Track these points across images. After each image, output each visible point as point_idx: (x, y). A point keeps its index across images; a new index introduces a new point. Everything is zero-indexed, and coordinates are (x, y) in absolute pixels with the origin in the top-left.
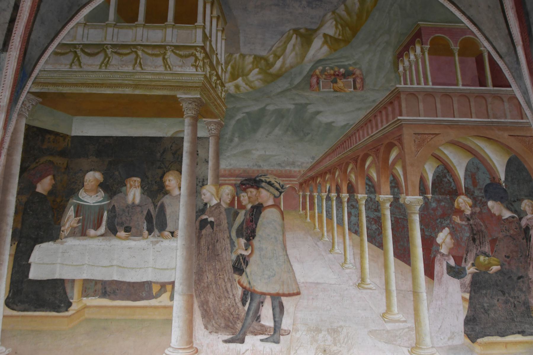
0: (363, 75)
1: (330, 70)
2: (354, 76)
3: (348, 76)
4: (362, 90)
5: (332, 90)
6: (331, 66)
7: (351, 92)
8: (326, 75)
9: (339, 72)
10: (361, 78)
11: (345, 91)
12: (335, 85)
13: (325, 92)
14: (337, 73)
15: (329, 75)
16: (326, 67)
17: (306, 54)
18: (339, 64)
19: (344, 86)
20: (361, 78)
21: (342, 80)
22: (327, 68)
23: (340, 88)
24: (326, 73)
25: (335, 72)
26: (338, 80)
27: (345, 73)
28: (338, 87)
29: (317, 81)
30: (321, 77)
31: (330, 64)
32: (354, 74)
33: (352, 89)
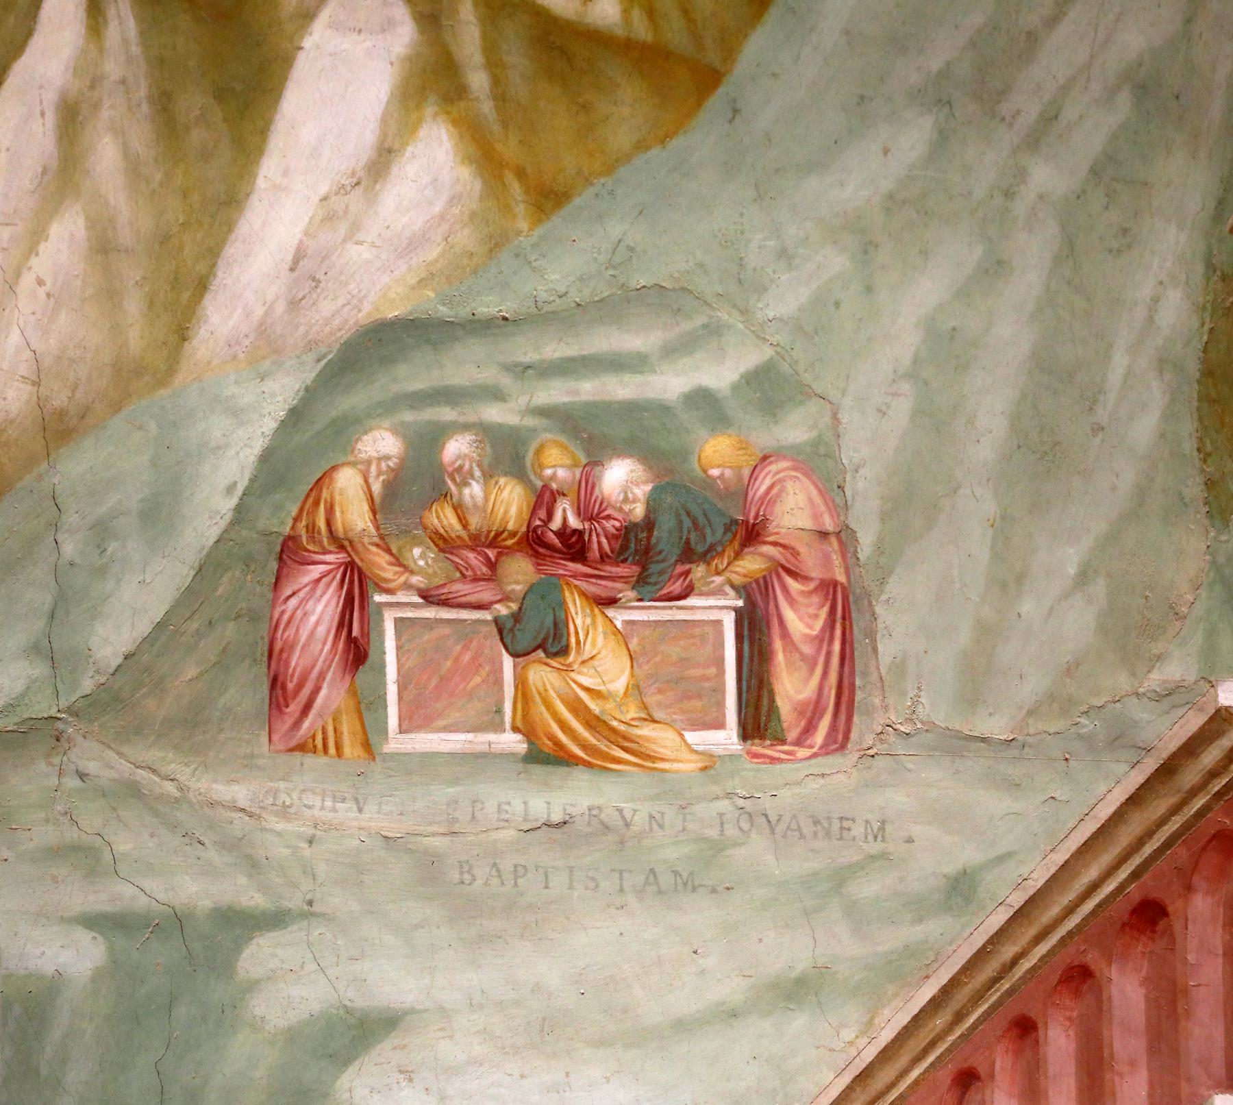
0: (844, 537)
1: (488, 476)
2: (751, 564)
3: (688, 555)
4: (839, 741)
5: (511, 741)
6: (494, 414)
7: (710, 763)
8: (444, 544)
9: (591, 510)
10: (829, 588)
11: (645, 756)
12: (542, 675)
13: (427, 759)
14: (566, 514)
15: (477, 541)
16: (436, 435)
17: (213, 253)
18: (587, 389)
19: (636, 689)
20: (829, 588)
21: (619, 617)
22: (456, 448)
23: (594, 723)
24: (445, 519)
25: (545, 499)
26: (579, 616)
27: (649, 524)
28: (577, 707)
29: (344, 622)
30: (379, 563)
31: (496, 395)
32: (751, 534)
33: (727, 738)
